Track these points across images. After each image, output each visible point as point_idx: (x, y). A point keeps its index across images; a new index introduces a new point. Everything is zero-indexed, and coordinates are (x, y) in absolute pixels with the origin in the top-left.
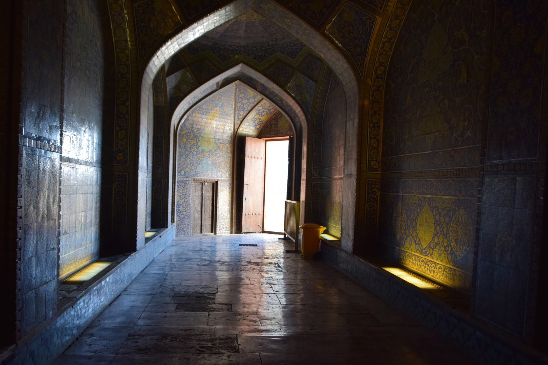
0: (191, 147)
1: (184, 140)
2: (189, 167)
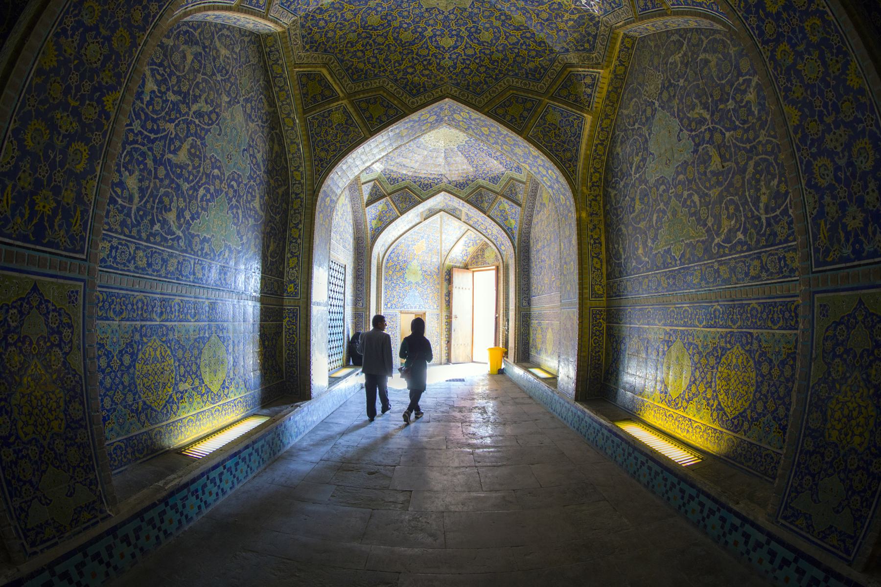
2: (396, 299)
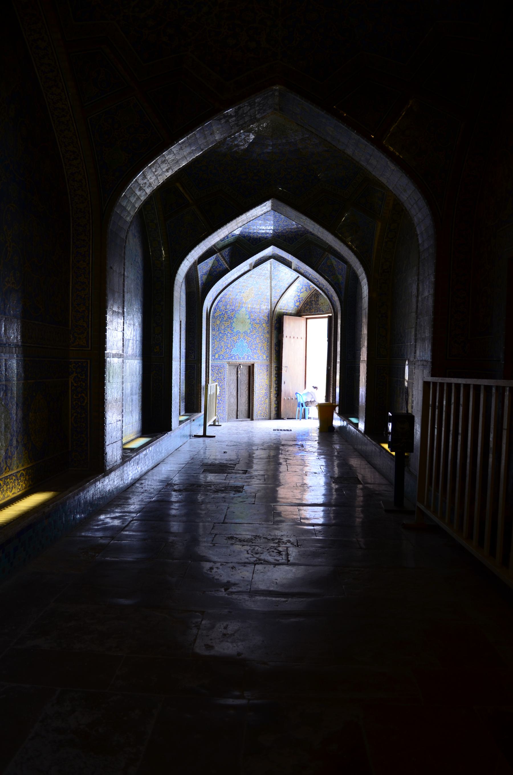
1: (218, 322)
2: (223, 350)
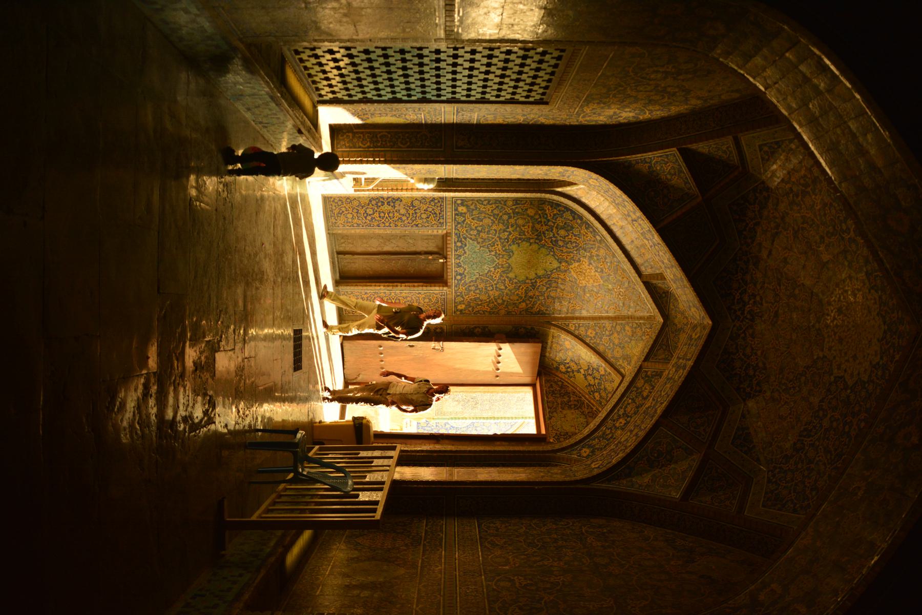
0: (518, 226)
1: (531, 212)
2: (475, 223)
